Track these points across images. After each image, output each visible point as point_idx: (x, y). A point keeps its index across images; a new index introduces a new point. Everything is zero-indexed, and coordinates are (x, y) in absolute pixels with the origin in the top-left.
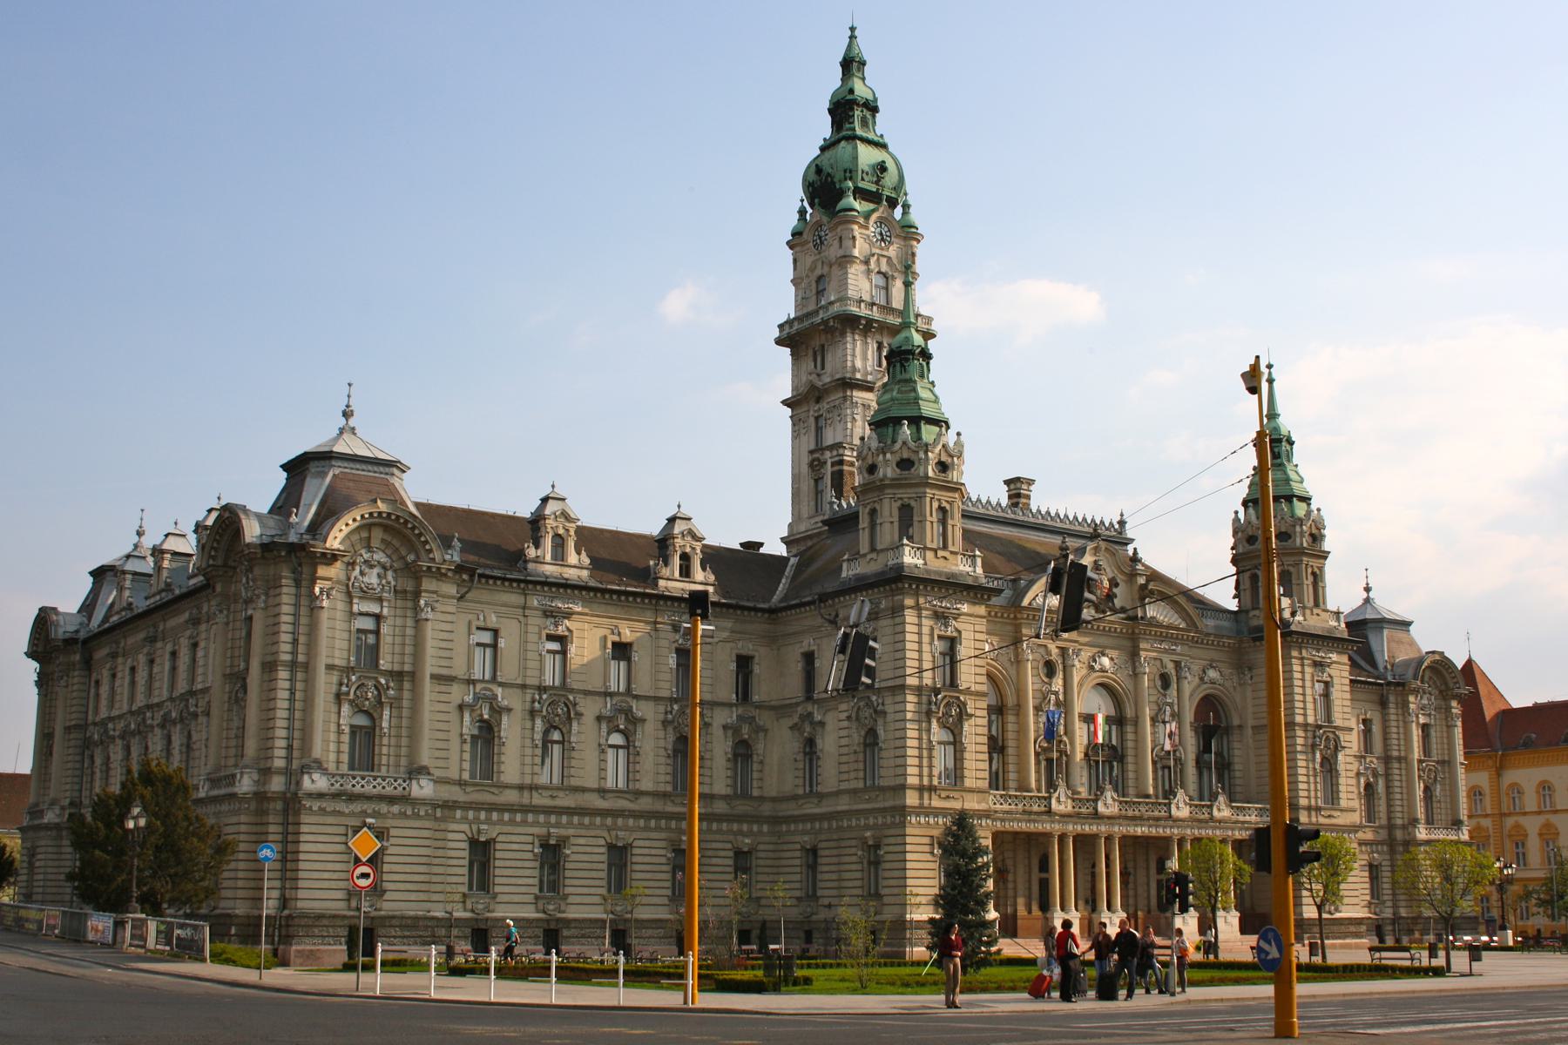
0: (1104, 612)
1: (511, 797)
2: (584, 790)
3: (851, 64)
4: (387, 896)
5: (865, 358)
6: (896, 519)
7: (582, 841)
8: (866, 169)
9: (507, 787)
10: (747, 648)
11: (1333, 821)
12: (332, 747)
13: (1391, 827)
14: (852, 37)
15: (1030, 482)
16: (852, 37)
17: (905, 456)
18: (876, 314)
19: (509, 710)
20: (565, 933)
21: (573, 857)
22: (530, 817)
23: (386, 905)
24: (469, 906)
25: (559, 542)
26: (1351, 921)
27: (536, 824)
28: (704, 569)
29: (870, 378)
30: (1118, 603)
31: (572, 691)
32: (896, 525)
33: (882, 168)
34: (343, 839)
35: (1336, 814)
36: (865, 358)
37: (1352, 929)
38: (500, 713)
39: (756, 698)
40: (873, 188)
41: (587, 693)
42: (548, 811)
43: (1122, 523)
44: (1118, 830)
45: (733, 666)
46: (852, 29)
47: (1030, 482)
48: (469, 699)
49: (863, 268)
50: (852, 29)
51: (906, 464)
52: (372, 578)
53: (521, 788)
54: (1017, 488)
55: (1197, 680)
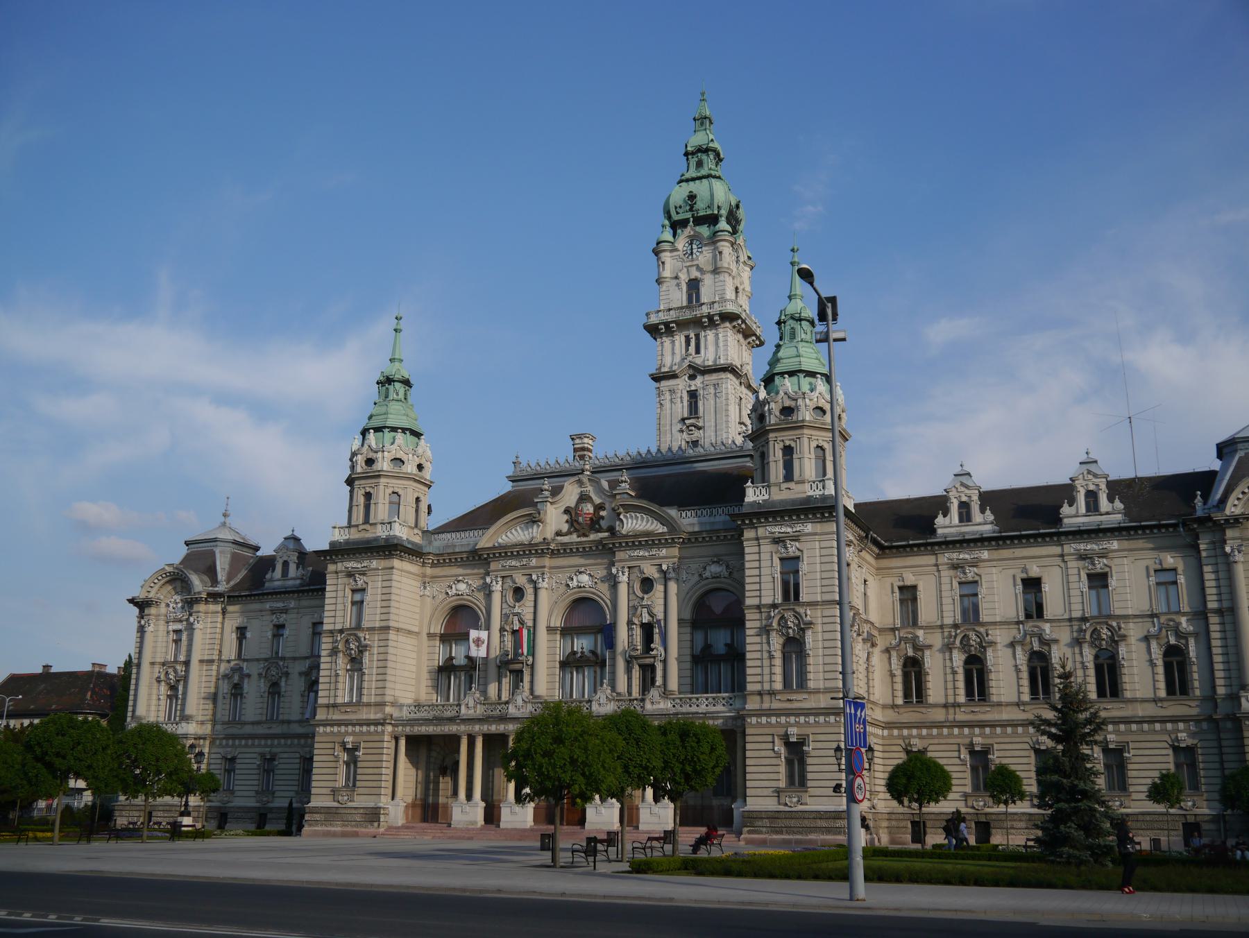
1: (248, 729)
2: (289, 722)
5: (673, 353)
7: (286, 755)
8: (680, 203)
9: (245, 723)
12: (153, 708)
13: (1210, 698)
19: (249, 676)
20: (269, 816)
22: (256, 742)
24: (970, 804)
25: (1092, 496)
26: (820, 815)
27: (259, 746)
28: (983, 511)
29: (675, 368)
31: (283, 659)
33: (692, 197)
34: (956, 754)
35: (800, 697)
36: (673, 353)
37: (823, 823)
38: (922, 650)
40: (689, 215)
41: (295, 659)
42: (266, 737)
48: (1153, 630)
49: (675, 282)
53: (253, 723)
55: (696, 578)
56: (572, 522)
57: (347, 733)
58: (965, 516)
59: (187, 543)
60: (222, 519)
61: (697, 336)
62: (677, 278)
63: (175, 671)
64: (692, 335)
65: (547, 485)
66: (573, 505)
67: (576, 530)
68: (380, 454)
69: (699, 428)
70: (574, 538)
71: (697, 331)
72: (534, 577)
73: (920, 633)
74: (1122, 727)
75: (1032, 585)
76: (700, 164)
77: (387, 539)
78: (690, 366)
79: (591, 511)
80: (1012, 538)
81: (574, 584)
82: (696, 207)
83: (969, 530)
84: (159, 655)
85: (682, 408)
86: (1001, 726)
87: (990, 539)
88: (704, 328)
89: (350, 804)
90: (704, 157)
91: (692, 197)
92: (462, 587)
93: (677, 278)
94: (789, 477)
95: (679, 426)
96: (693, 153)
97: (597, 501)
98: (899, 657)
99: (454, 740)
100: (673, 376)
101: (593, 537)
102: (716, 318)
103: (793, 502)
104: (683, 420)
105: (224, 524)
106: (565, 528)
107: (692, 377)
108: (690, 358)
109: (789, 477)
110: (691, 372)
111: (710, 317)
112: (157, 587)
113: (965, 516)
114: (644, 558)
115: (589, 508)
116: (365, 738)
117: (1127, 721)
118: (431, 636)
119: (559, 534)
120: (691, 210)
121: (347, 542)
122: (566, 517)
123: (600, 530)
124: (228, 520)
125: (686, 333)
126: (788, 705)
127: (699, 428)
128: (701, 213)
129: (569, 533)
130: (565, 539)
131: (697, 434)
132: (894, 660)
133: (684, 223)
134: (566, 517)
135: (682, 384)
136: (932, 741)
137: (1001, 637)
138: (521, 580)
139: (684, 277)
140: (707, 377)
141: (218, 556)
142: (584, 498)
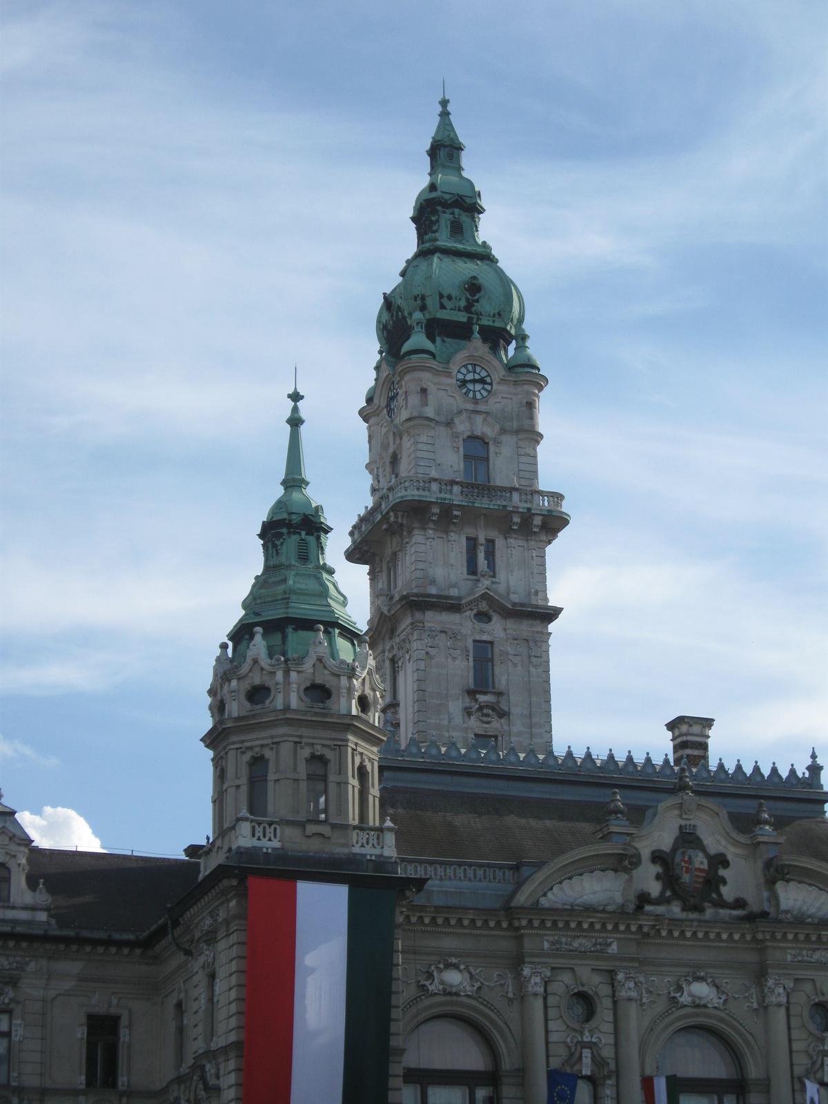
0: (701, 910)
6: (244, 781)
10: (100, 1002)
14: (445, 114)
15: (708, 723)
16: (445, 114)
18: (456, 496)
30: (728, 892)
33: (474, 287)
39: (122, 1080)
40: (462, 317)
43: (815, 769)
45: (81, 1032)
46: (444, 103)
47: (708, 723)
50: (444, 103)
54: (690, 734)
56: (669, 878)
61: (491, 543)
62: (449, 424)
64: (482, 540)
65: (619, 799)
67: (676, 896)
69: (503, 714)
70: (676, 909)
71: (492, 534)
72: (620, 976)
76: (457, 229)
78: (485, 597)
79: (705, 866)
81: (685, 999)
82: (477, 307)
85: (460, 669)
87: (46, 938)
88: (507, 531)
90: (464, 218)
91: (474, 287)
92: (454, 978)
93: (449, 424)
95: (468, 702)
96: (446, 205)
97: (712, 851)
100: (454, 607)
101: (709, 912)
102: (537, 521)
104: (472, 693)
106: (655, 888)
107: (483, 617)
108: (486, 582)
110: (484, 606)
119: (643, 899)
120: (468, 308)
123: (721, 903)
125: (470, 531)
127: (503, 714)
129: (661, 900)
130: (660, 909)
131: (496, 725)
133: (460, 332)
135: (466, 625)
138: (594, 983)
139: (462, 427)
140: (510, 624)
142: (688, 839)
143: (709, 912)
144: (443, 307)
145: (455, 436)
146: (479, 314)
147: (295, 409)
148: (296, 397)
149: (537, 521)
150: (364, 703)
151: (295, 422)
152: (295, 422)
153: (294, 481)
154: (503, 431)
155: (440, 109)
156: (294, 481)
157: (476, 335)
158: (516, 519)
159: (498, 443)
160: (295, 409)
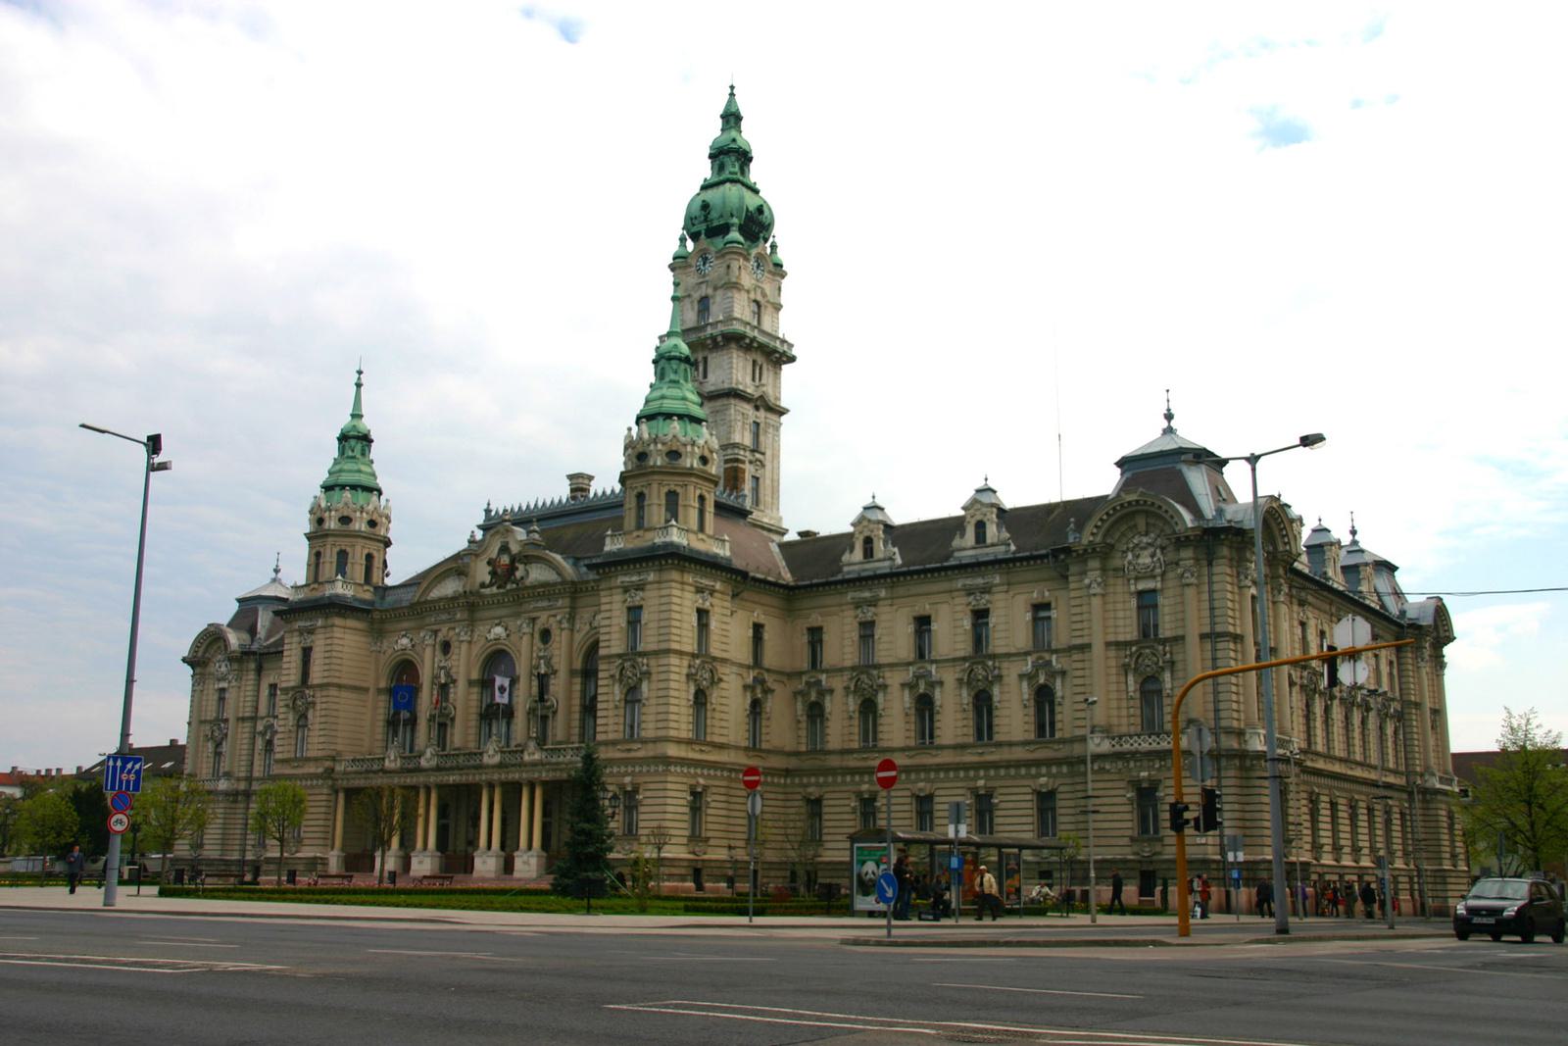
3: (732, 118)
4: (207, 847)
11: (632, 754)
14: (732, 95)
16: (732, 95)
17: (345, 514)
21: (1003, 805)
23: (205, 853)
32: (334, 565)
33: (705, 206)
35: (635, 746)
44: (433, 779)
46: (732, 87)
50: (732, 87)
51: (345, 520)
52: (223, 669)
55: (587, 627)
56: (493, 573)
57: (626, 774)
58: (868, 552)
59: (239, 601)
60: (273, 575)
61: (705, 360)
63: (220, 729)
66: (494, 555)
68: (327, 514)
71: (706, 353)
73: (823, 677)
74: (992, 772)
75: (923, 623)
77: (329, 598)
80: (918, 572)
81: (491, 636)
83: (872, 567)
84: (209, 713)
86: (1025, 766)
89: (298, 855)
93: (689, 296)
94: (640, 526)
98: (803, 703)
99: (378, 792)
102: (719, 339)
103: (641, 550)
105: (274, 580)
106: (487, 579)
109: (640, 526)
111: (713, 338)
112: (204, 646)
113: (868, 552)
114: (544, 609)
115: (505, 559)
116: (309, 792)
117: (996, 765)
118: (379, 691)
119: (483, 585)
120: (706, 220)
121: (301, 602)
122: (489, 568)
124: (280, 575)
126: (624, 755)
128: (715, 224)
129: (491, 585)
130: (487, 591)
132: (799, 706)
134: (489, 568)
136: (939, 785)
137: (894, 679)
139: (696, 296)
141: (260, 613)
143: (509, 587)
144: (694, 225)
145: (692, 302)
146: (712, 220)
147: (359, 378)
148: (360, 372)
149: (719, 339)
150: (704, 460)
151: (359, 385)
152: (359, 385)
153: (357, 415)
154: (715, 289)
155: (729, 91)
156: (357, 415)
157: (703, 236)
158: (709, 342)
159: (713, 297)
160: (359, 378)
